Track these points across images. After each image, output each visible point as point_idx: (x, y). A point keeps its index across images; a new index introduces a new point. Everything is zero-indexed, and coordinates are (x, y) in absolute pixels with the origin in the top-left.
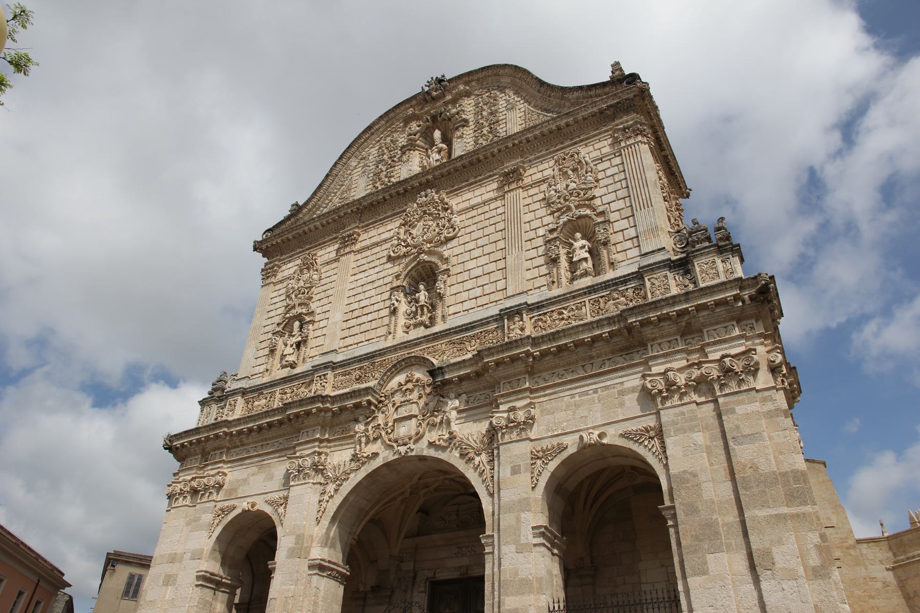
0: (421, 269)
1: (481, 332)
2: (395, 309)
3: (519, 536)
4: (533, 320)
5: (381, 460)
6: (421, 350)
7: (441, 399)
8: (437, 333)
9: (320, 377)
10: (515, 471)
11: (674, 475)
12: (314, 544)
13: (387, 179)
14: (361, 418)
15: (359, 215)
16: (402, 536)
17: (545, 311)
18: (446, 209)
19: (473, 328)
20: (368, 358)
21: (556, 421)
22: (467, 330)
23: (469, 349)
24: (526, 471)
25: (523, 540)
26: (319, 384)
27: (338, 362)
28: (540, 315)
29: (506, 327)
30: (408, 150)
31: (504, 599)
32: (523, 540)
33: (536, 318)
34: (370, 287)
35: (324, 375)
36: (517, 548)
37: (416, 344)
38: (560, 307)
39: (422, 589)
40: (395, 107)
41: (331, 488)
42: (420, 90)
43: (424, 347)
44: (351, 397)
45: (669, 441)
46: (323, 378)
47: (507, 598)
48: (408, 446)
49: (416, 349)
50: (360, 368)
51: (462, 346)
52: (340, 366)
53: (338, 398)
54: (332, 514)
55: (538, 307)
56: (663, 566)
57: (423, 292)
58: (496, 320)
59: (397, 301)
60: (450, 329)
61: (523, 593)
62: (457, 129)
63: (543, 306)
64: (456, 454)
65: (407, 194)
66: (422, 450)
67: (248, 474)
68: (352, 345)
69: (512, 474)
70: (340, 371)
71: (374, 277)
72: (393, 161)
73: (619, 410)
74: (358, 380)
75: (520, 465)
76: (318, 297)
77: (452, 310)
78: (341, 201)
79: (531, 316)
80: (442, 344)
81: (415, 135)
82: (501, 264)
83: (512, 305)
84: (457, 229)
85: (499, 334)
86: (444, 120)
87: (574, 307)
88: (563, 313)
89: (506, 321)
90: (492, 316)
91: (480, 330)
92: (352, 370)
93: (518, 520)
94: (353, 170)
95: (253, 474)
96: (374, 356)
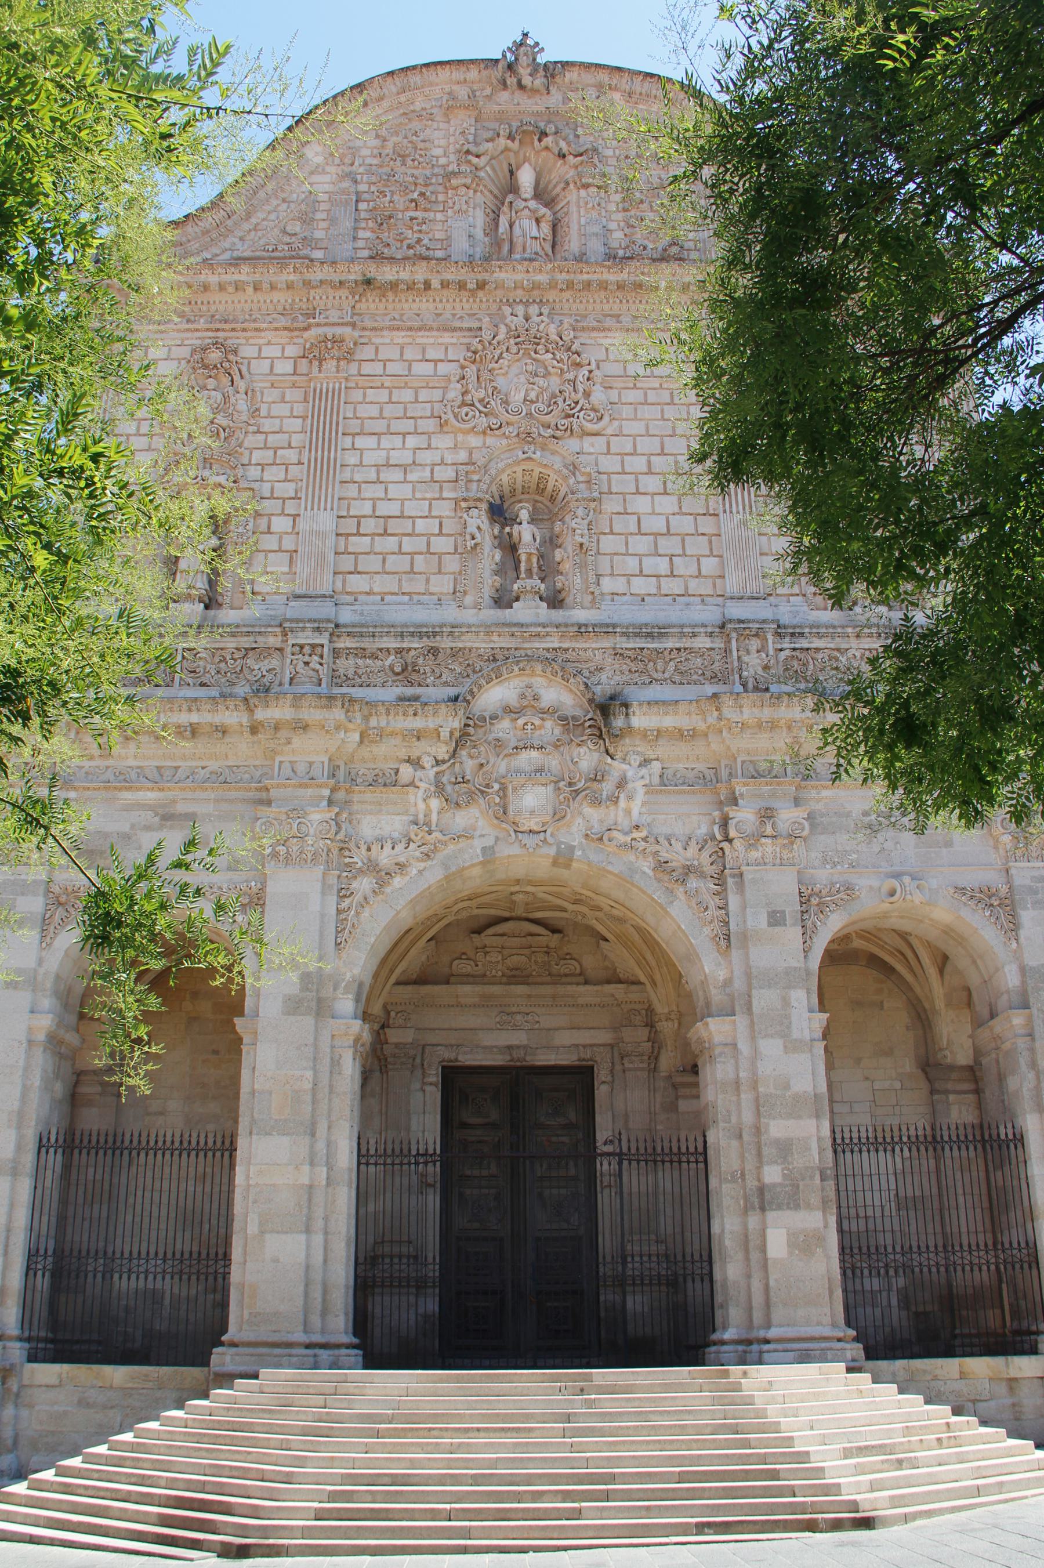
0: (519, 474)
1: (679, 650)
2: (476, 545)
3: (789, 1027)
4: (783, 655)
5: (479, 851)
6: (548, 650)
7: (609, 760)
8: (586, 625)
9: (302, 647)
10: (776, 919)
11: (1031, 968)
12: (339, 993)
13: (409, 233)
14: (427, 762)
15: (357, 297)
16: (393, 979)
17: (806, 645)
18: (579, 365)
19: (661, 635)
20: (421, 635)
21: (840, 848)
22: (650, 635)
23: (655, 676)
24: (794, 925)
25: (795, 1034)
26: (301, 665)
27: (345, 626)
28: (794, 649)
29: (735, 653)
30: (465, 185)
31: (768, 1125)
32: (795, 1034)
33: (787, 653)
34: (397, 475)
35: (313, 646)
36: (785, 1047)
37: (538, 635)
38: (832, 646)
39: (433, 1079)
40: (427, 65)
41: (364, 885)
42: (500, 57)
43: (556, 645)
44: (415, 714)
45: (1026, 916)
46: (307, 650)
47: (772, 1123)
48: (542, 836)
49: (537, 645)
50: (399, 651)
51: (641, 666)
52: (349, 634)
53: (382, 709)
54: (373, 939)
55: (792, 634)
56: (867, 1079)
57: (525, 524)
58: (711, 635)
59: (479, 528)
60: (614, 626)
61: (800, 1117)
62: (586, 186)
63: (802, 634)
64: (646, 866)
65: (480, 294)
66: (572, 849)
67: (133, 826)
68: (367, 593)
69: (770, 924)
70: (349, 645)
71: (406, 457)
72: (422, 194)
73: (944, 850)
74: (398, 674)
75: (783, 912)
76: (257, 456)
77: (608, 585)
78: (287, 239)
79: (779, 647)
80: (594, 649)
81: (478, 156)
82: (707, 525)
83: (750, 616)
84: (606, 418)
85: (717, 664)
86: (547, 148)
87: (858, 654)
88: (837, 659)
89: (734, 643)
90: (704, 626)
91: (678, 645)
92: (381, 650)
93: (786, 1002)
94: (312, 173)
95: (148, 828)
96: (435, 634)
